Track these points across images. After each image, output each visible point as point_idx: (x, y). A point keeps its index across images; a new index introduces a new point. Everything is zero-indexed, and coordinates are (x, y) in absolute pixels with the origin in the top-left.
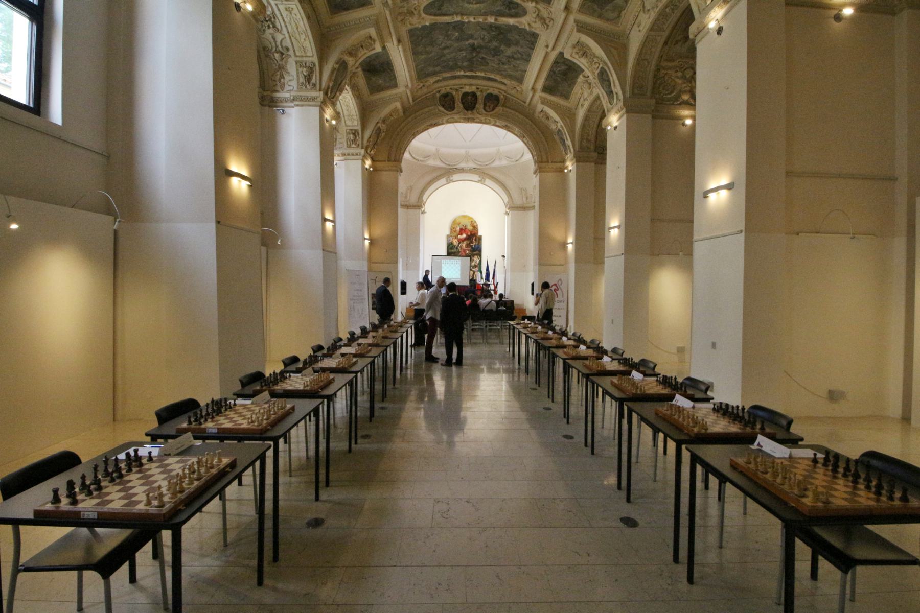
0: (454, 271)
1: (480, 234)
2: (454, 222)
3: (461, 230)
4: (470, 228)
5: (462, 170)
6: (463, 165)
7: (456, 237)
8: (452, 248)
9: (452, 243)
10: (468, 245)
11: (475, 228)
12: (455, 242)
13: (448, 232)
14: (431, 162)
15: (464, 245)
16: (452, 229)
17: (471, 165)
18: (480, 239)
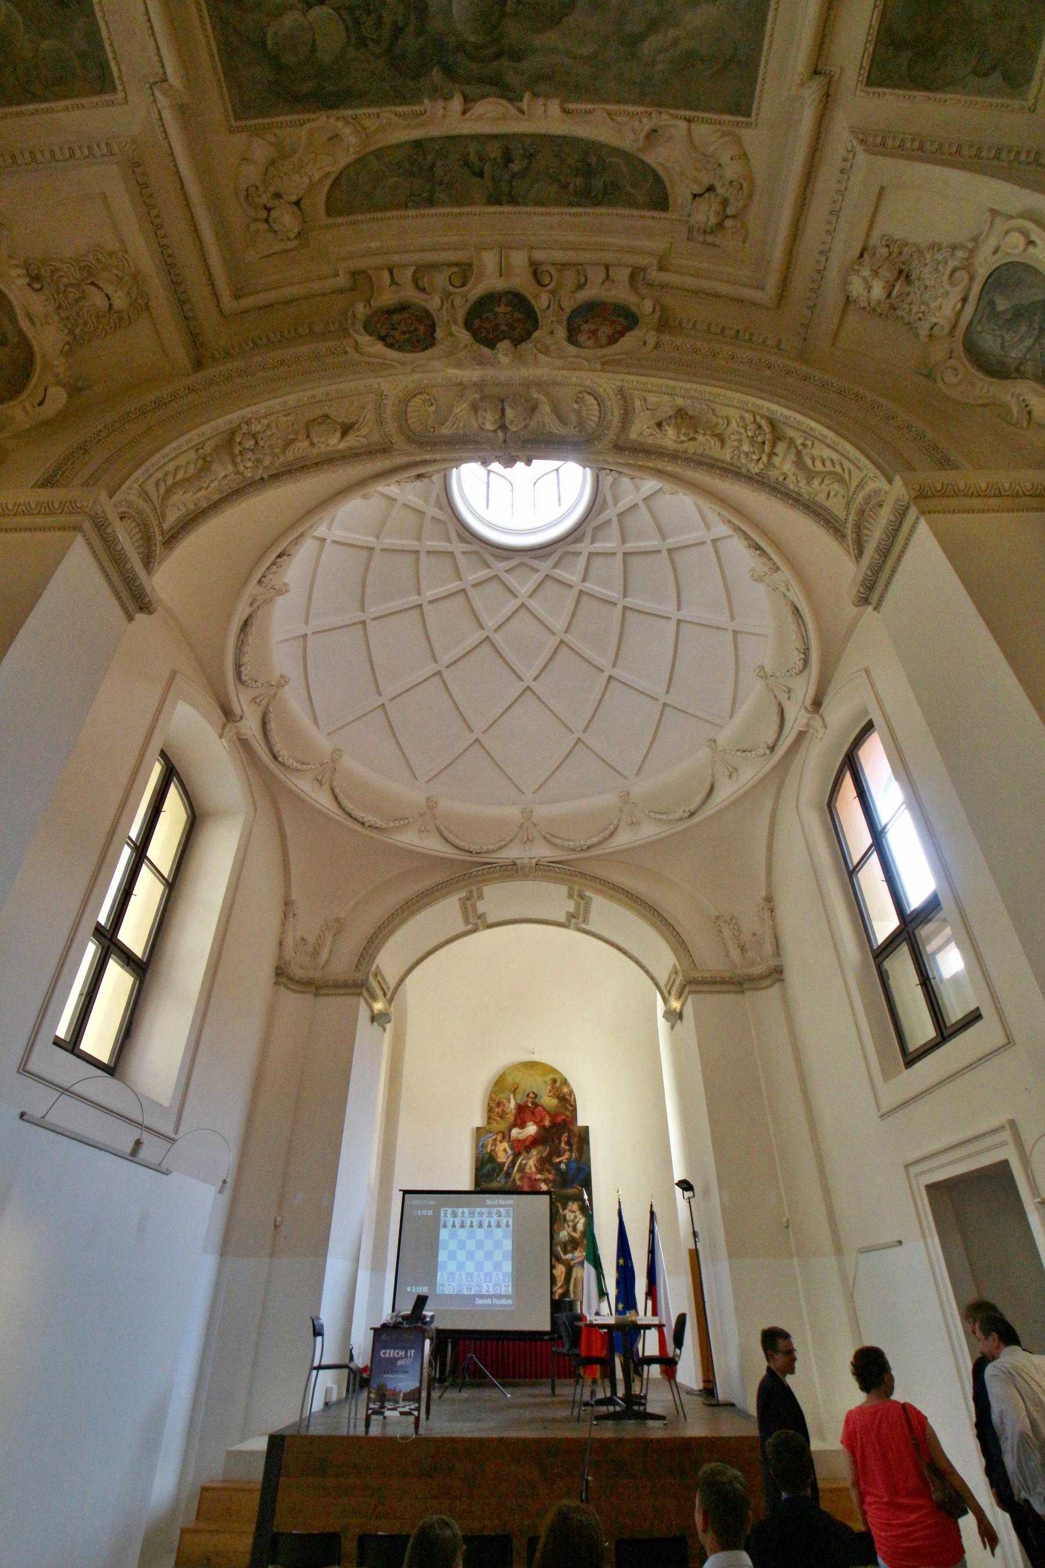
0: (484, 1271)
1: (581, 1122)
2: (500, 1084)
3: (521, 1109)
4: (549, 1101)
5: (512, 871)
6: (513, 853)
7: (505, 1136)
8: (490, 1176)
9: (491, 1158)
10: (544, 1163)
11: (566, 1101)
12: (503, 1153)
13: (478, 1120)
14: (409, 838)
15: (531, 1162)
16: (494, 1108)
17: (542, 852)
18: (583, 1137)
